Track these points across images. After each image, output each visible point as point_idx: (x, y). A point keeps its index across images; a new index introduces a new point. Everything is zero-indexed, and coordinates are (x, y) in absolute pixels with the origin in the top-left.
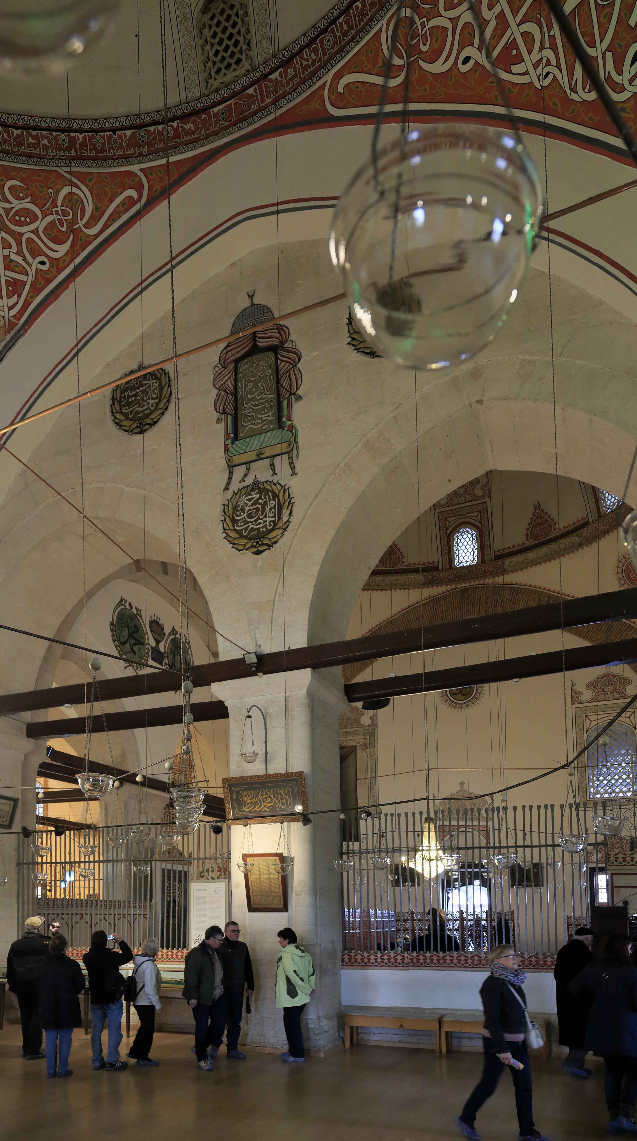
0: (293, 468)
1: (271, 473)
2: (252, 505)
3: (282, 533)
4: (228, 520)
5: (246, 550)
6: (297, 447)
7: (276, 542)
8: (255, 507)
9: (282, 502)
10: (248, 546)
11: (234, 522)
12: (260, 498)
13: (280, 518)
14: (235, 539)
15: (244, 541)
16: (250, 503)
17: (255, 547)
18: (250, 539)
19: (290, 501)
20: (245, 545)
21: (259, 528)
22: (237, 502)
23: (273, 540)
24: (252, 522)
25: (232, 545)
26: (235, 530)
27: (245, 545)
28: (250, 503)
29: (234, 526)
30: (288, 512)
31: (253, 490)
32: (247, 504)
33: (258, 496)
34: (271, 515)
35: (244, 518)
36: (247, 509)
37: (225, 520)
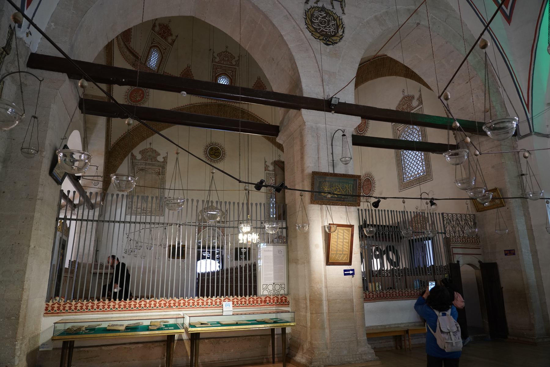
0: (343, 10)
1: (332, 7)
2: (322, 18)
3: (339, 40)
4: (308, 19)
5: (320, 40)
6: (344, 2)
7: (336, 43)
8: (324, 20)
9: (339, 25)
10: (321, 38)
11: (312, 22)
12: (326, 16)
13: (338, 32)
14: (313, 31)
15: (318, 35)
16: (321, 17)
17: (325, 40)
18: (322, 35)
19: (342, 26)
20: (319, 37)
21: (326, 32)
22: (313, 13)
23: (335, 41)
24: (323, 27)
25: (311, 34)
26: (313, 26)
27: (319, 37)
28: (321, 17)
29: (312, 24)
30: (342, 31)
31: (322, 10)
32: (319, 17)
33: (325, 15)
34: (333, 28)
35: (318, 22)
36: (319, 19)
37: (306, 19)
